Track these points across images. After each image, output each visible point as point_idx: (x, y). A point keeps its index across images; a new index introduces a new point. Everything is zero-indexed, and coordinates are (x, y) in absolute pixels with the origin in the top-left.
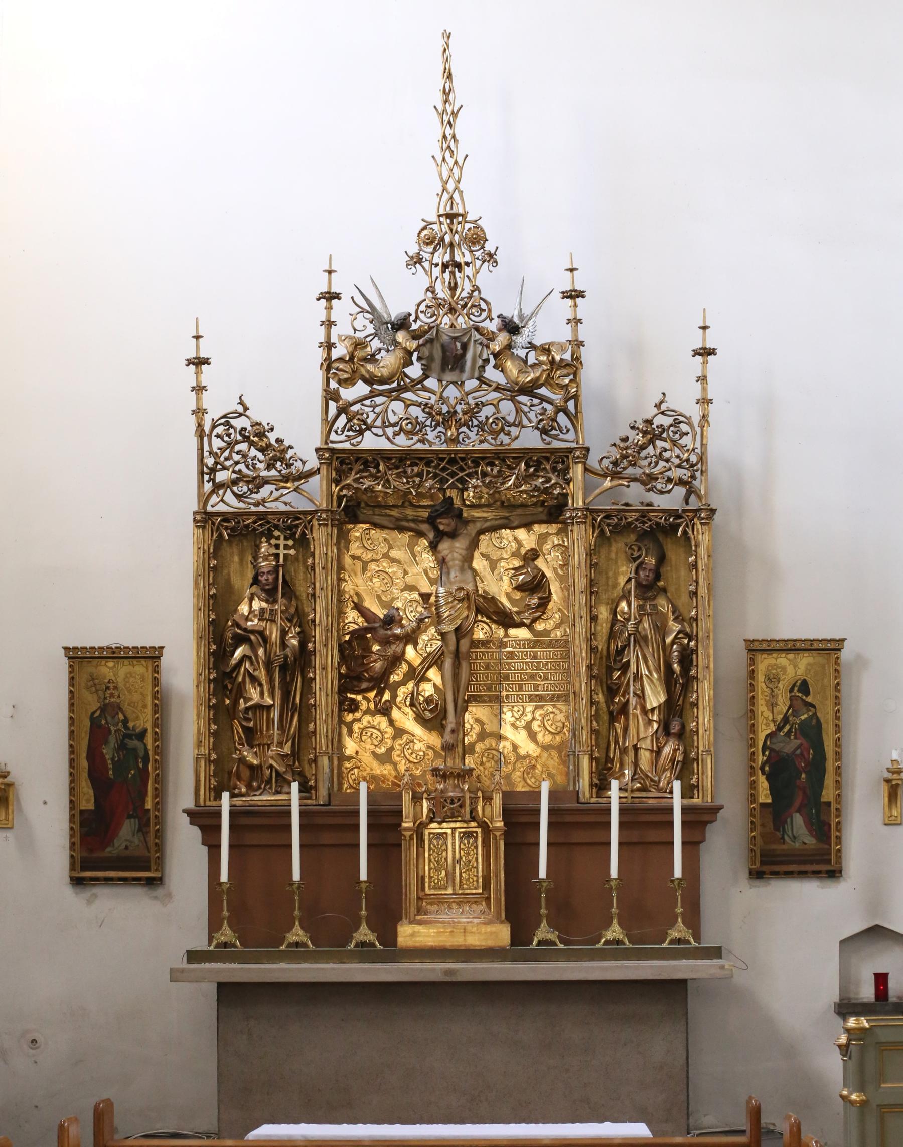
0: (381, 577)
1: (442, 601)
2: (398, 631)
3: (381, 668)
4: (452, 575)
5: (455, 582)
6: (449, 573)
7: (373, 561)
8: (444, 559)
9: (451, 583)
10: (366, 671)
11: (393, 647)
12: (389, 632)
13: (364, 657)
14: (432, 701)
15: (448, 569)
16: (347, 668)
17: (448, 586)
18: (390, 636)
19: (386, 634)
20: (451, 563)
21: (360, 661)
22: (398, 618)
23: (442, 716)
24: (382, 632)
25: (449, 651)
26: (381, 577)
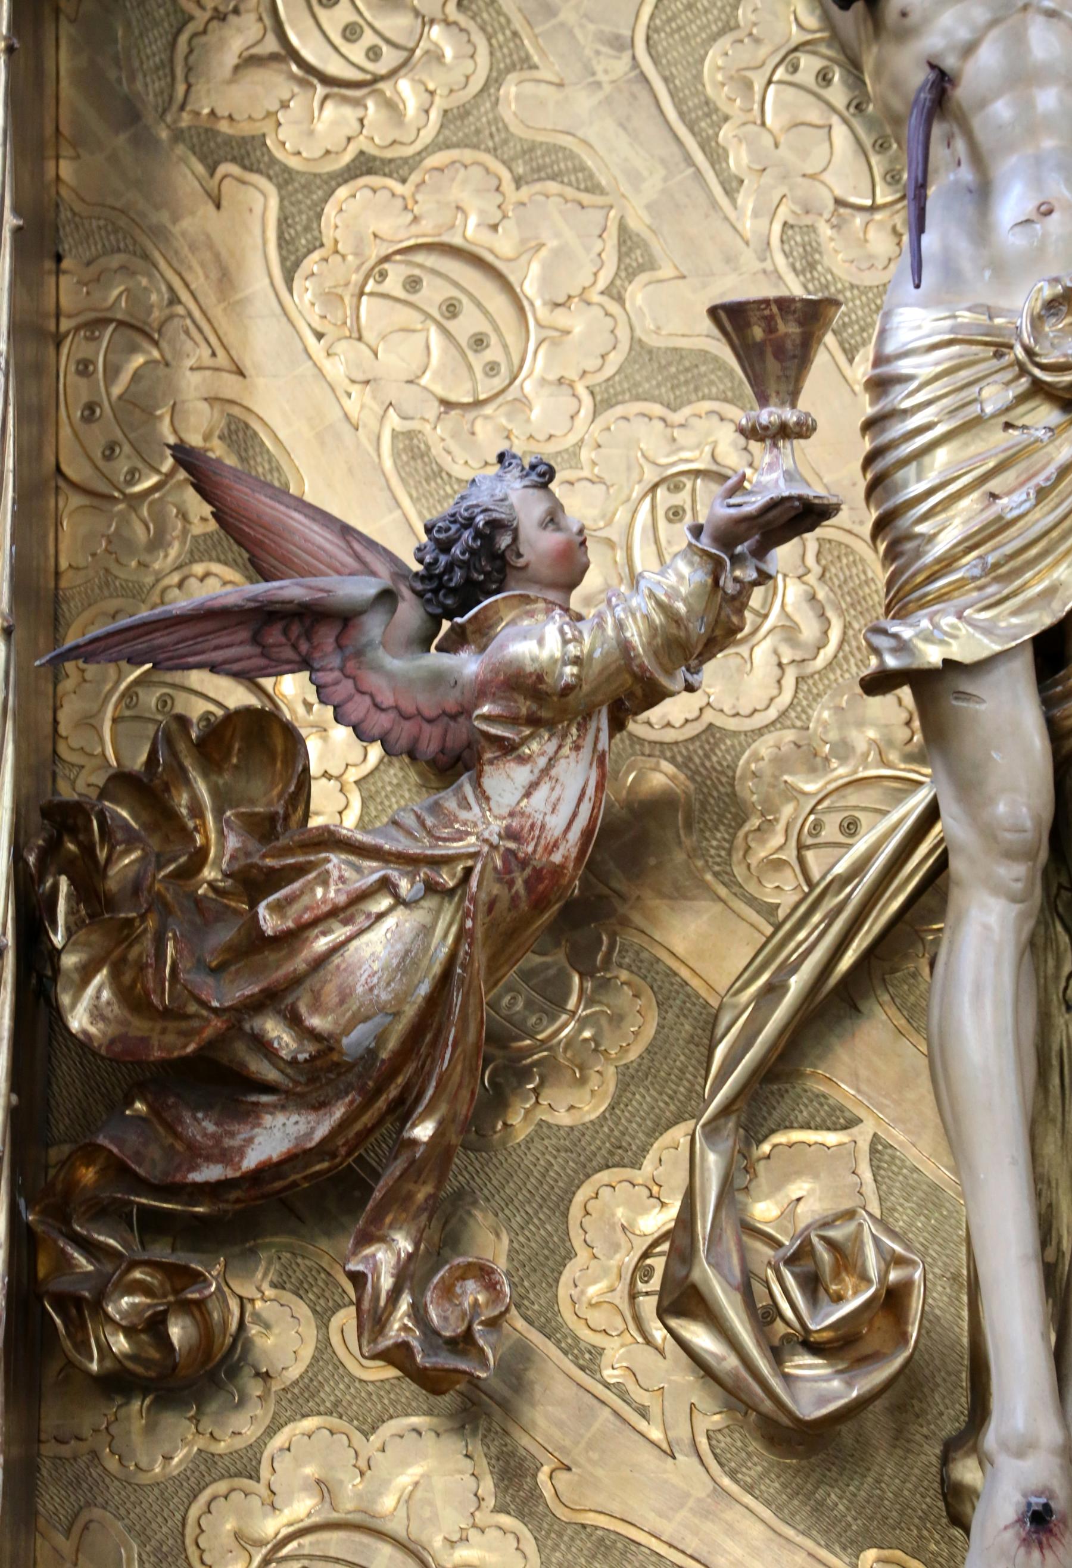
0: (433, 293)
1: (924, 410)
2: (535, 640)
3: (407, 963)
4: (1012, 204)
5: (1037, 254)
6: (983, 193)
7: (365, 165)
8: (942, 82)
9: (1000, 269)
10: (271, 999)
11: (505, 782)
12: (468, 664)
13: (255, 883)
14: (846, 1257)
15: (978, 159)
16: (132, 998)
17: (982, 290)
18: (482, 690)
19: (438, 679)
20: (1002, 109)
21: (224, 935)
22: (538, 544)
23: (949, 1412)
24: (399, 665)
25: (988, 833)
26: (433, 293)
